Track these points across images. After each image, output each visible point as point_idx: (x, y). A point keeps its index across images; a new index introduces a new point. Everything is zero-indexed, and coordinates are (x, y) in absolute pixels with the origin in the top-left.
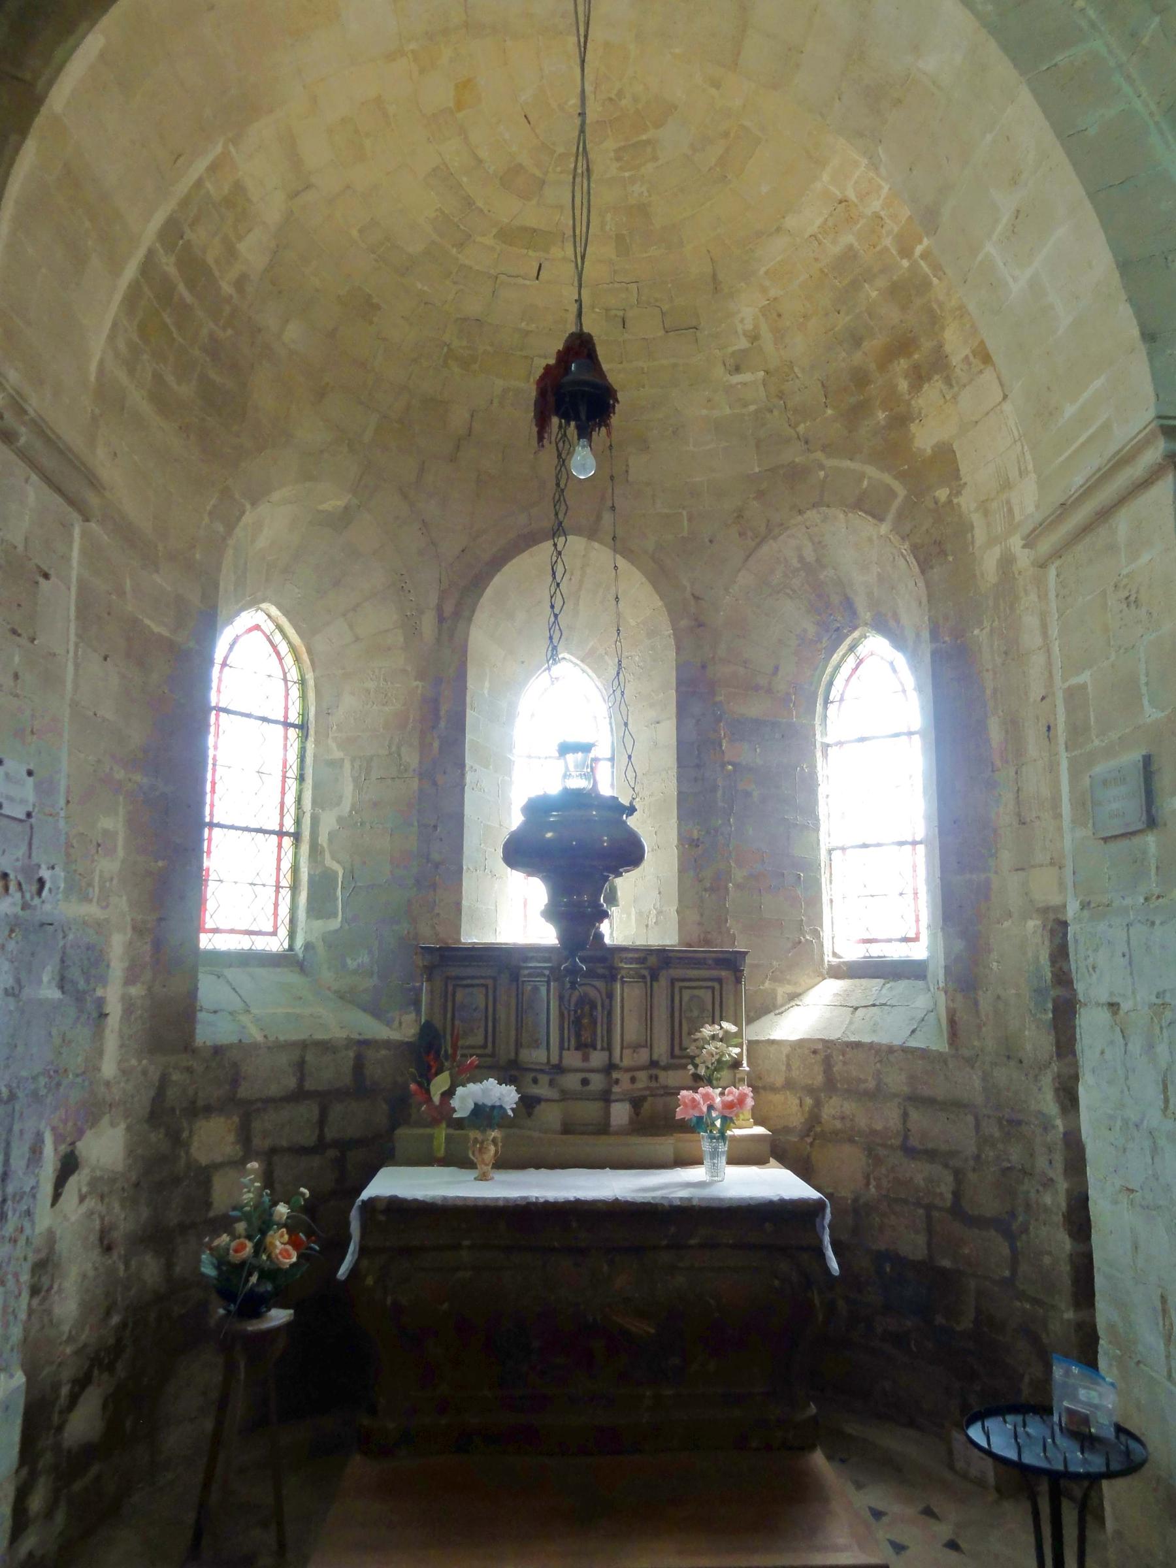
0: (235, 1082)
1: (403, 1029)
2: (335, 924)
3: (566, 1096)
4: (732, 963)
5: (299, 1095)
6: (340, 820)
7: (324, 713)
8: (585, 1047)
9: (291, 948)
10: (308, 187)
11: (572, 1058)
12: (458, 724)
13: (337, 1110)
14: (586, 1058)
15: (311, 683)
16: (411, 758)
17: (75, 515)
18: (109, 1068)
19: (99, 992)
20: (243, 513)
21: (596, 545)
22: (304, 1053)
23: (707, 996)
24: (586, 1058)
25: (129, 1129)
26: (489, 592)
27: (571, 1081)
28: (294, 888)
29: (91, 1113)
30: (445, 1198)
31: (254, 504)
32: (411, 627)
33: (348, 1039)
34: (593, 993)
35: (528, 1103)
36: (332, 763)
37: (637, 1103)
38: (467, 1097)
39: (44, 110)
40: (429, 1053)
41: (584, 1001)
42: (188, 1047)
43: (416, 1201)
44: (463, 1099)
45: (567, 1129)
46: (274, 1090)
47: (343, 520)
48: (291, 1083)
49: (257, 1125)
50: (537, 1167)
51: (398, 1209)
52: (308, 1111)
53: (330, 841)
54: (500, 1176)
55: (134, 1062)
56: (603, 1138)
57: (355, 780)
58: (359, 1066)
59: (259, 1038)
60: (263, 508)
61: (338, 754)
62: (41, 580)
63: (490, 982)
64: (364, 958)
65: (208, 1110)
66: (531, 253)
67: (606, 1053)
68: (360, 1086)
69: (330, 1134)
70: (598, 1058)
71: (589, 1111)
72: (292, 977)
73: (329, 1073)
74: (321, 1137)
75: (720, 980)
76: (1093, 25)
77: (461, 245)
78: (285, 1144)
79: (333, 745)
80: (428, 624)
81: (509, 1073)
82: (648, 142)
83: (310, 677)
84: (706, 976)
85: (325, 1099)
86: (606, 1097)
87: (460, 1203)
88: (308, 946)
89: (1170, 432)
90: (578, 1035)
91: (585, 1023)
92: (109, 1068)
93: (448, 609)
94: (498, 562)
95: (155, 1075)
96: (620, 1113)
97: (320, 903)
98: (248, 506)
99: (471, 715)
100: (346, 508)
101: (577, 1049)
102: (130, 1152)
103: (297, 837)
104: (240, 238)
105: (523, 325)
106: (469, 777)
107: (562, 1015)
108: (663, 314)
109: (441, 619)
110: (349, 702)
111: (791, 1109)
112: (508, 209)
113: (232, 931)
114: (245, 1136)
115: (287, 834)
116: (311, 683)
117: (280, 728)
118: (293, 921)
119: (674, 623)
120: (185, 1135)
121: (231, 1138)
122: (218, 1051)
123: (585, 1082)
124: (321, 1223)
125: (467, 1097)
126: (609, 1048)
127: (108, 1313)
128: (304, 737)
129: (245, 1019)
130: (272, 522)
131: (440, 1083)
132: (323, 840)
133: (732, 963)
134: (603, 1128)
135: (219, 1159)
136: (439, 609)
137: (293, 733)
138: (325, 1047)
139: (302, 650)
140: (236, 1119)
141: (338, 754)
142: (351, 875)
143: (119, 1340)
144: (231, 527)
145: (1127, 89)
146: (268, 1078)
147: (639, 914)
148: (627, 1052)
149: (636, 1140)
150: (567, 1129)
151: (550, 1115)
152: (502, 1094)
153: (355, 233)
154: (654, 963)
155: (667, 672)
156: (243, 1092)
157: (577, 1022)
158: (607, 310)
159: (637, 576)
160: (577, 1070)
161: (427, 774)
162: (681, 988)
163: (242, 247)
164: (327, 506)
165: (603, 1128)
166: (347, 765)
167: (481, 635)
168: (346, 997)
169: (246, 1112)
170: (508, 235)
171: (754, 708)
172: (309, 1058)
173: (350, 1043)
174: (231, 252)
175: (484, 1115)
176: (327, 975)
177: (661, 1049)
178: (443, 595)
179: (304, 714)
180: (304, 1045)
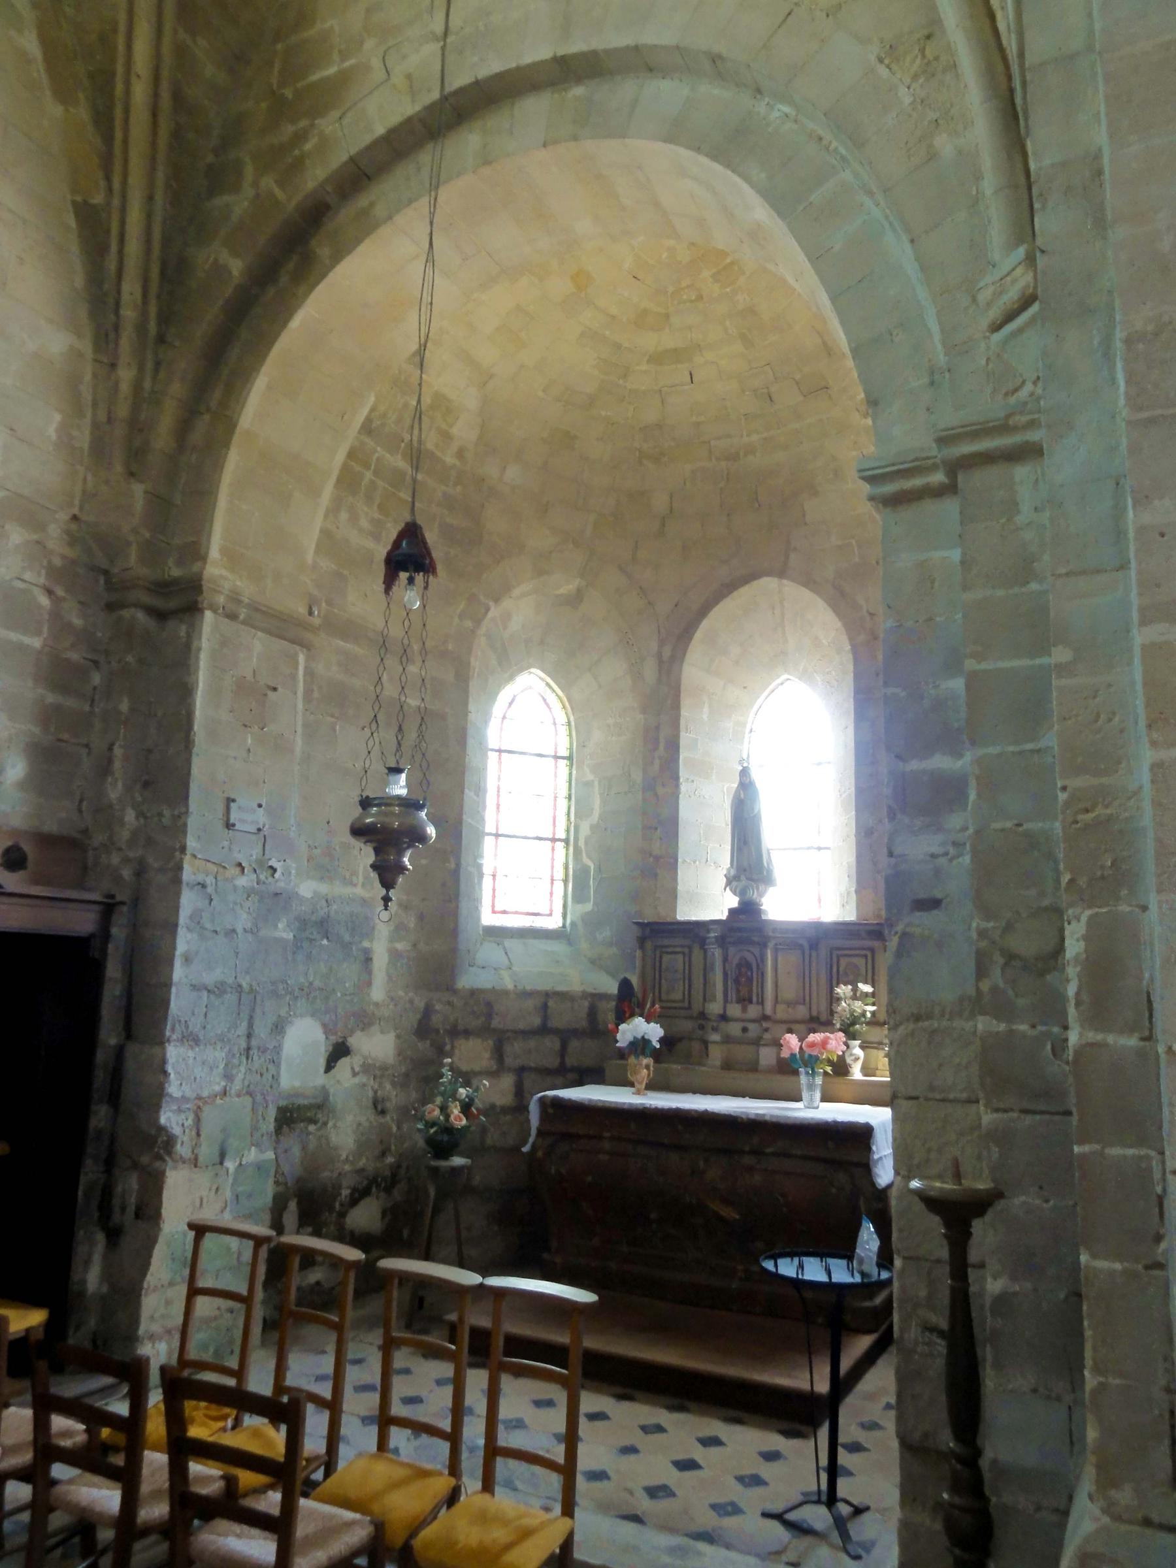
0: (489, 1016)
2: (589, 907)
3: (728, 1040)
5: (544, 1030)
6: (592, 827)
7: (582, 745)
8: (745, 1001)
9: (564, 926)
10: (491, 376)
11: (734, 1010)
12: (674, 746)
13: (574, 1044)
14: (744, 1010)
15: (573, 723)
16: (637, 776)
17: (298, 648)
18: (378, 993)
19: (366, 944)
20: (488, 610)
21: (785, 582)
22: (546, 1000)
23: (861, 962)
24: (744, 1010)
25: (398, 1037)
26: (698, 635)
27: (734, 1029)
28: (566, 881)
29: (365, 1020)
30: (590, 1100)
31: (497, 600)
33: (584, 992)
34: (750, 958)
36: (589, 784)
39: (238, 430)
41: (744, 965)
42: (451, 989)
43: (570, 1100)
44: (624, 1032)
45: (727, 1066)
46: (521, 1026)
47: (577, 599)
48: (537, 1021)
49: (508, 1049)
50: (694, 1093)
52: (552, 1043)
53: (586, 843)
54: (650, 1094)
55: (401, 993)
56: (751, 1075)
57: (601, 794)
58: (592, 1013)
59: (510, 986)
60: (507, 603)
61: (590, 777)
62: (270, 693)
63: (686, 950)
64: (606, 933)
65: (467, 1033)
66: (679, 366)
67: (760, 1007)
69: (570, 1061)
70: (753, 1011)
73: (561, 1019)
74: (562, 1063)
75: (872, 950)
76: (843, 158)
77: (625, 376)
78: (533, 1065)
79: (587, 770)
80: (650, 671)
82: (732, 263)
83: (572, 718)
85: (566, 1036)
87: (600, 1104)
88: (573, 924)
89: (872, 480)
90: (738, 991)
92: (378, 993)
93: (667, 652)
94: (704, 611)
95: (420, 1004)
97: (580, 894)
98: (491, 604)
99: (685, 738)
100: (579, 590)
101: (738, 1002)
102: (400, 1053)
103: (567, 841)
104: (451, 426)
105: (694, 418)
106: (683, 788)
107: (725, 975)
108: (797, 383)
109: (661, 662)
112: (650, 341)
113: (516, 913)
114: (499, 1053)
115: (560, 840)
116: (573, 723)
117: (552, 760)
118: (565, 906)
119: (851, 639)
120: (448, 1047)
121: (487, 1055)
122: (473, 993)
123: (745, 1030)
126: (762, 1002)
127: (383, 1154)
128: (571, 766)
129: (505, 974)
130: (519, 611)
132: (581, 843)
134: (753, 1067)
135: (477, 1068)
136: (659, 655)
137: (563, 764)
138: (562, 996)
139: (565, 699)
140: (491, 1042)
141: (590, 777)
142: (599, 869)
143: (394, 1175)
144: (478, 622)
145: (868, 202)
148: (781, 1008)
149: (779, 1078)
150: (727, 1066)
152: (654, 1032)
153: (541, 394)
156: (496, 1023)
157: (737, 981)
158: (755, 391)
159: (821, 604)
160: (737, 1020)
161: (649, 787)
162: (838, 957)
163: (454, 431)
164: (561, 591)
165: (753, 1067)
166: (596, 783)
167: (692, 671)
170: (658, 358)
172: (551, 1003)
173: (585, 995)
174: (447, 436)
175: (640, 1046)
176: (584, 945)
178: (662, 643)
179: (571, 749)
180: (547, 995)
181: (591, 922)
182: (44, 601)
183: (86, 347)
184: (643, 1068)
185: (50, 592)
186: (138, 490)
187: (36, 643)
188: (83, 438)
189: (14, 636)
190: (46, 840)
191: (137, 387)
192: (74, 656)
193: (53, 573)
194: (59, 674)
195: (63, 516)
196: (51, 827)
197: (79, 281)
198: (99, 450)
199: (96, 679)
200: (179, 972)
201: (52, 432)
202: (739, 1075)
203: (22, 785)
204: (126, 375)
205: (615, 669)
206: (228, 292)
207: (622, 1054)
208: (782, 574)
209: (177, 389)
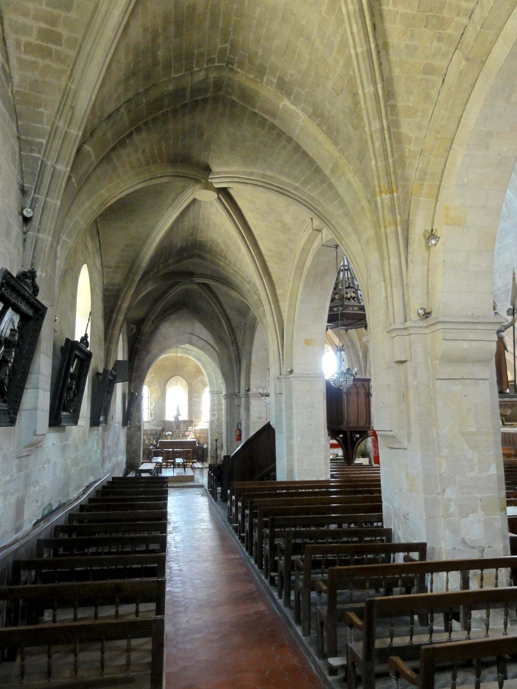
1: (160, 428)
4: (192, 421)
5: (151, 434)
8: (178, 429)
22: (152, 430)
32: (160, 387)
35: (172, 435)
37: (183, 435)
38: (167, 433)
40: (163, 430)
41: (178, 425)
47: (153, 377)
51: (162, 442)
68: (156, 434)
71: (178, 435)
72: (148, 423)
73: (154, 432)
81: (171, 431)
84: (189, 423)
85: (153, 435)
86: (180, 434)
91: (178, 427)
94: (169, 380)
96: (181, 435)
97: (151, 416)
110: (153, 395)
111: (198, 435)
124: (157, 442)
125: (167, 433)
131: (164, 433)
133: (192, 421)
146: (149, 433)
147: (184, 417)
151: (175, 436)
152: (171, 433)
154: (185, 422)
155: (187, 390)
167: (167, 387)
168: (154, 425)
169: (147, 435)
171: (197, 395)
175: (169, 435)
177: (185, 430)
181: (153, 420)
184: (169, 437)
202: (179, 437)
205: (157, 386)
207: (166, 436)
208: (179, 376)
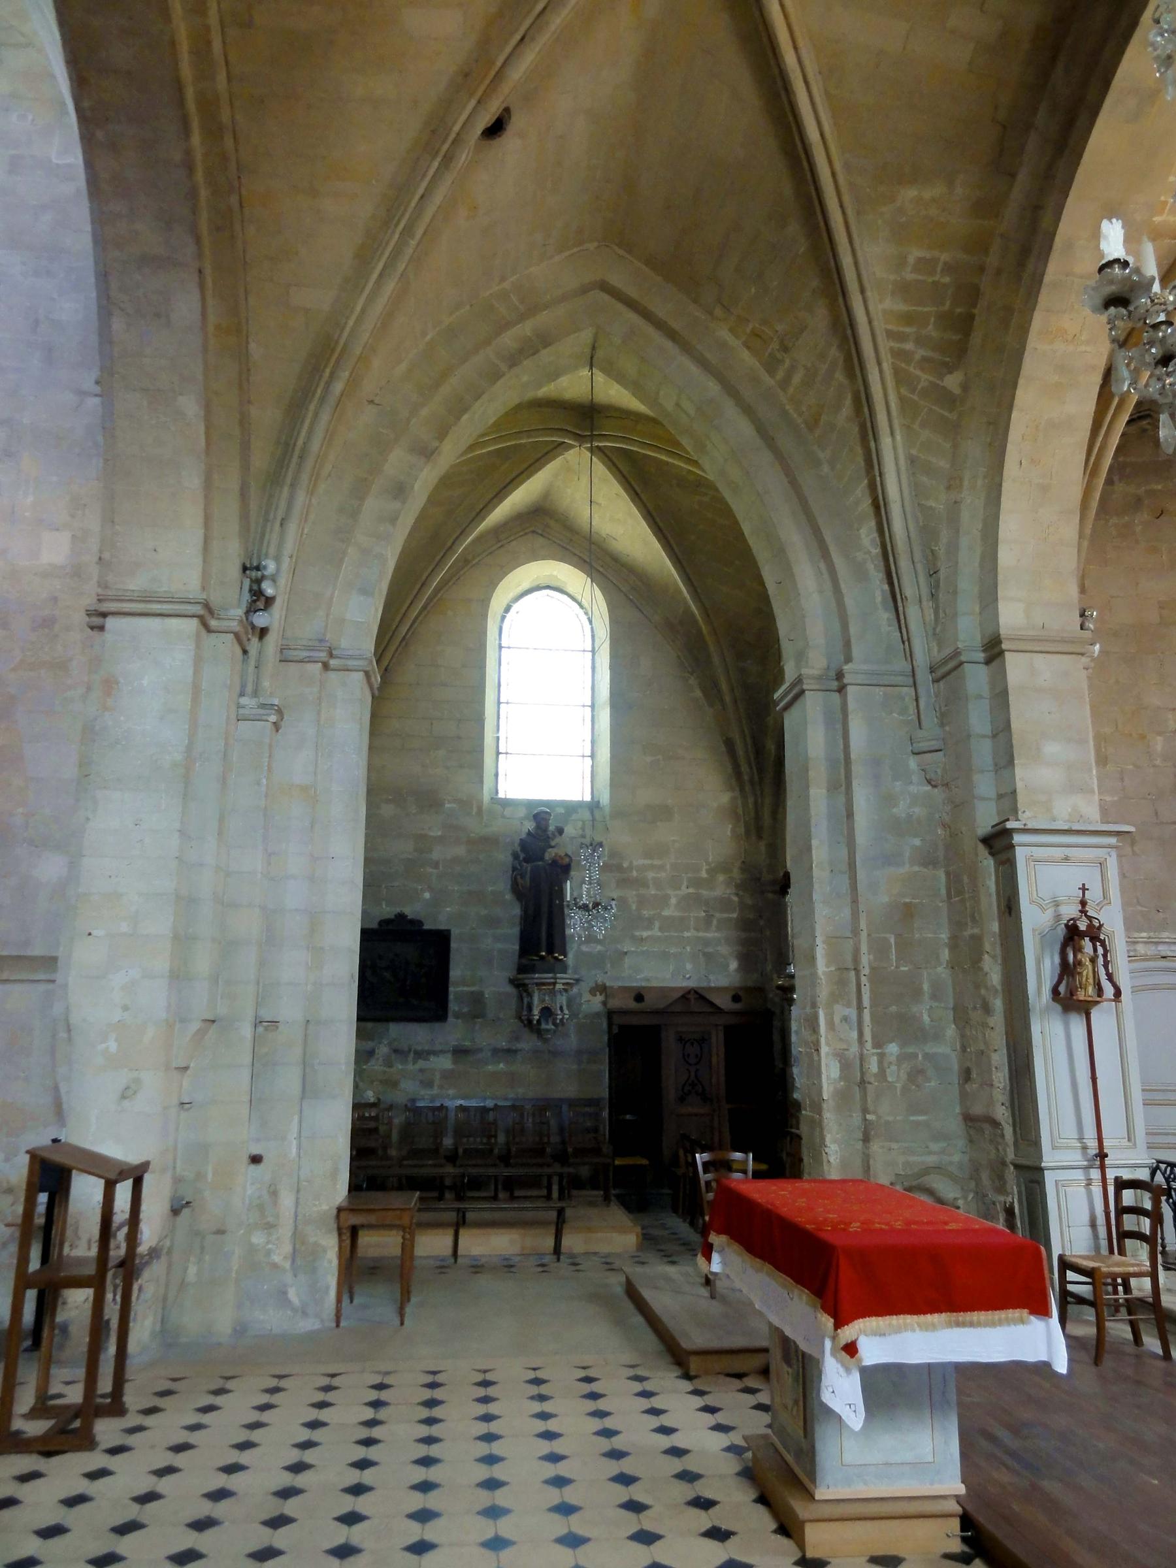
182: (736, 899)
183: (737, 793)
185: (737, 895)
186: (762, 846)
187: (735, 915)
188: (742, 830)
189: (726, 915)
190: (748, 990)
191: (756, 803)
192: (751, 916)
193: (737, 886)
194: (746, 925)
195: (738, 864)
196: (750, 984)
197: (730, 770)
198: (748, 832)
199: (762, 923)
200: (794, 1038)
201: (729, 833)
203: (737, 970)
204: (751, 800)
206: (772, 759)
209: (768, 801)
